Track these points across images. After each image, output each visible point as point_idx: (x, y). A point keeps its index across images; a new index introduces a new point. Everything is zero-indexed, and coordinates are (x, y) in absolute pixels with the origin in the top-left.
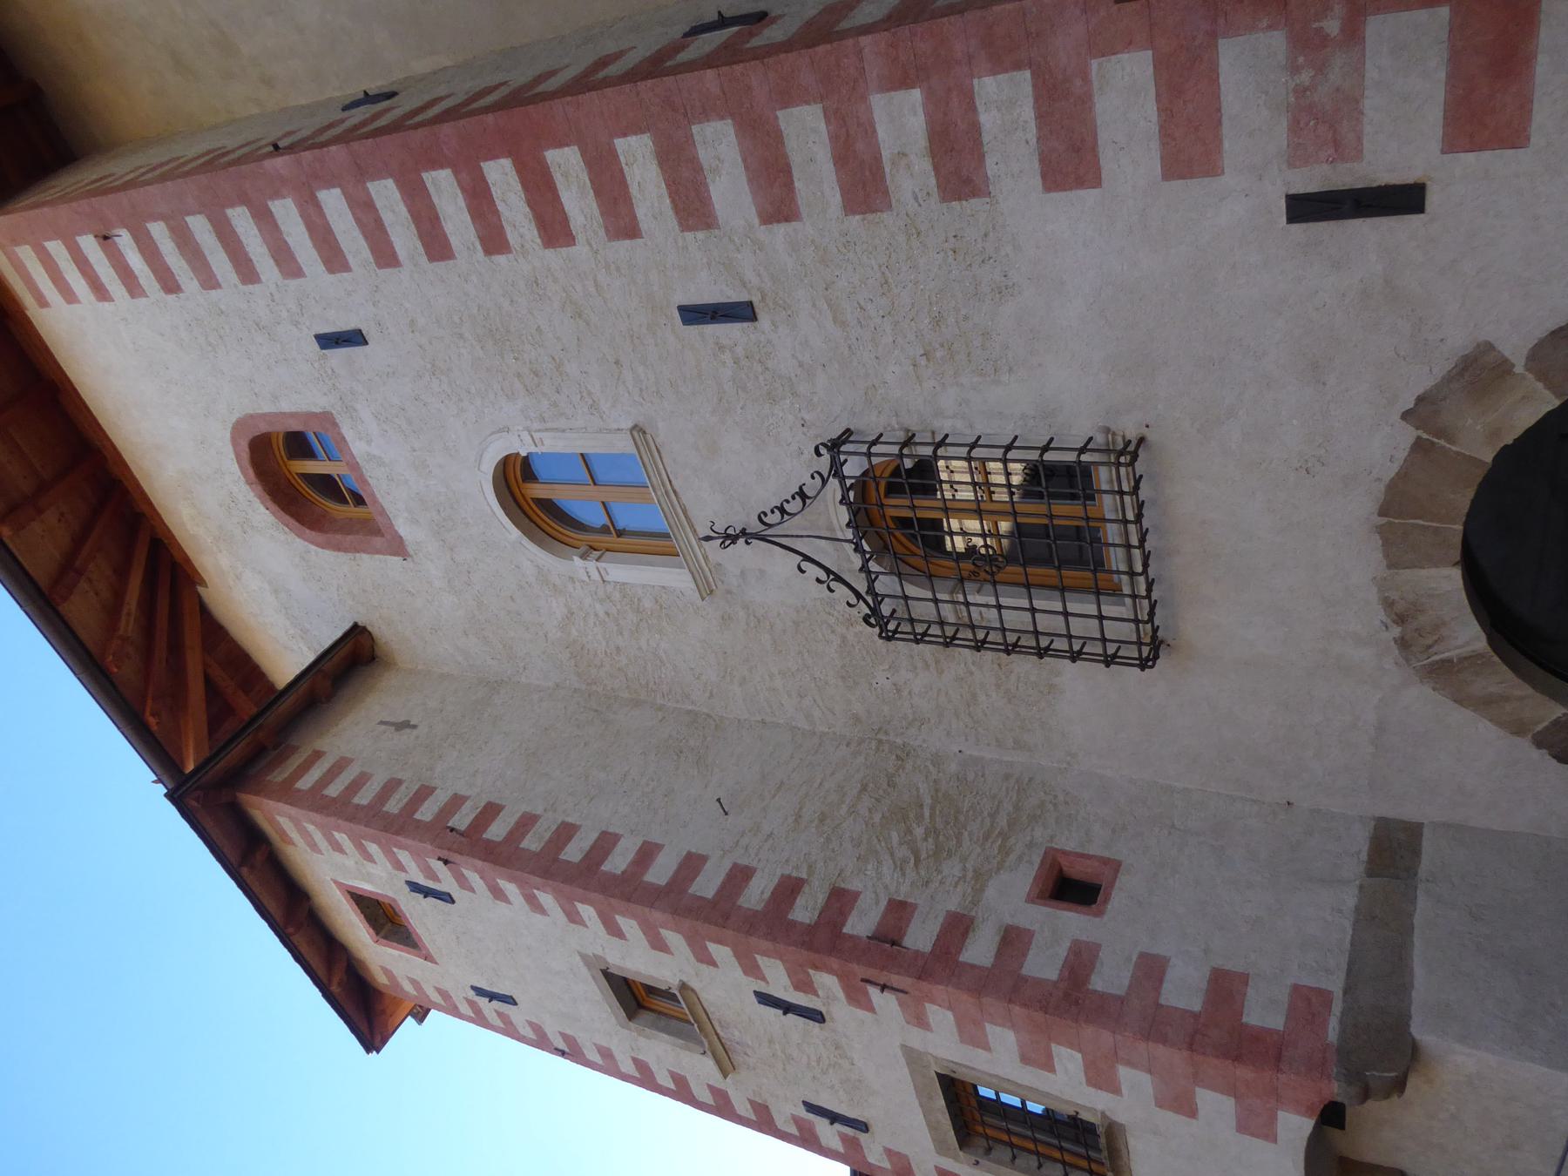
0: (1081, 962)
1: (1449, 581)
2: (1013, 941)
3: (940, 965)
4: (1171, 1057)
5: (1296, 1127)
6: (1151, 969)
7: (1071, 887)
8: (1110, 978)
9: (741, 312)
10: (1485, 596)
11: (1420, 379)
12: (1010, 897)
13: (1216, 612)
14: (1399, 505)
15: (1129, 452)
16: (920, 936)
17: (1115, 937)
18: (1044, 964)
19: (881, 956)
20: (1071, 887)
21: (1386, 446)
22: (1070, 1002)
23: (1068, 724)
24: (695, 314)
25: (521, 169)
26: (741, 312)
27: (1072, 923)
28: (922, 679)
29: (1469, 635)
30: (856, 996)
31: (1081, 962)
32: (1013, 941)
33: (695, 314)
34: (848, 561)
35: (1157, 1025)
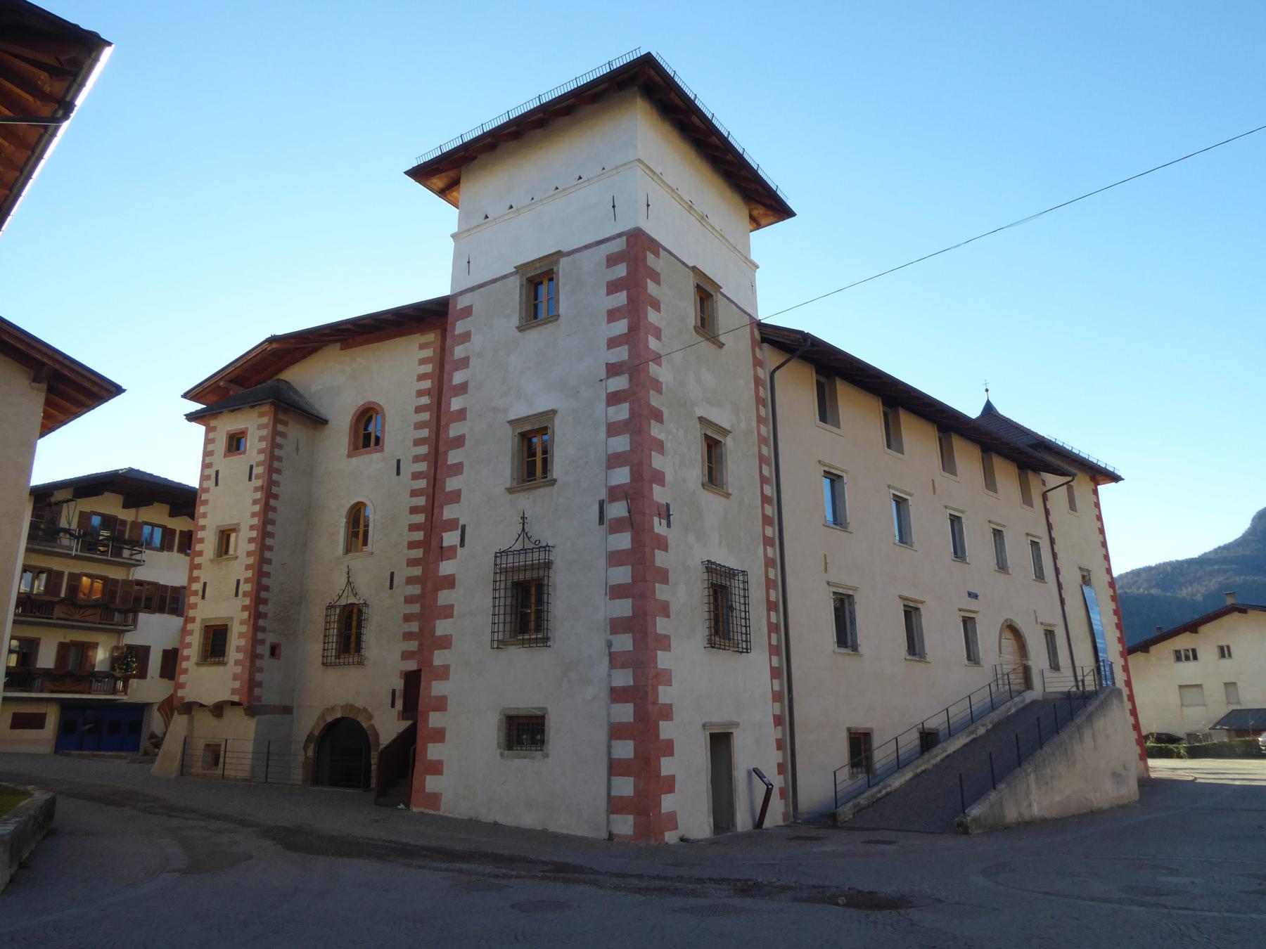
0: (261, 656)
1: (339, 715)
2: (262, 642)
3: (256, 628)
4: (246, 677)
5: (236, 699)
6: (261, 670)
7: (274, 650)
8: (259, 663)
9: (391, 587)
10: (337, 722)
11: (369, 710)
12: (270, 639)
13: (333, 675)
14: (351, 707)
15: (361, 663)
16: (261, 622)
17: (266, 662)
18: (259, 650)
19: (257, 615)
20: (274, 650)
21: (360, 705)
22: (254, 656)
23: (313, 644)
24: (392, 574)
25: (419, 542)
26: (391, 587)
27: (267, 653)
28: (318, 612)
29: (329, 719)
30: (244, 608)
31: (261, 656)
32: (262, 642)
33: (392, 574)
34: (343, 602)
35: (251, 674)
